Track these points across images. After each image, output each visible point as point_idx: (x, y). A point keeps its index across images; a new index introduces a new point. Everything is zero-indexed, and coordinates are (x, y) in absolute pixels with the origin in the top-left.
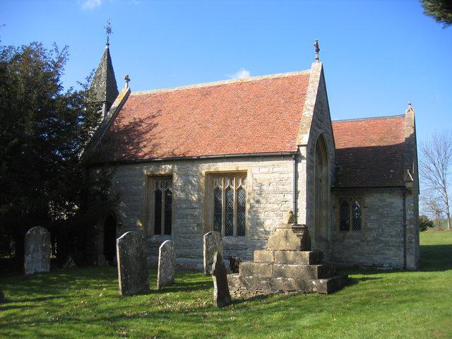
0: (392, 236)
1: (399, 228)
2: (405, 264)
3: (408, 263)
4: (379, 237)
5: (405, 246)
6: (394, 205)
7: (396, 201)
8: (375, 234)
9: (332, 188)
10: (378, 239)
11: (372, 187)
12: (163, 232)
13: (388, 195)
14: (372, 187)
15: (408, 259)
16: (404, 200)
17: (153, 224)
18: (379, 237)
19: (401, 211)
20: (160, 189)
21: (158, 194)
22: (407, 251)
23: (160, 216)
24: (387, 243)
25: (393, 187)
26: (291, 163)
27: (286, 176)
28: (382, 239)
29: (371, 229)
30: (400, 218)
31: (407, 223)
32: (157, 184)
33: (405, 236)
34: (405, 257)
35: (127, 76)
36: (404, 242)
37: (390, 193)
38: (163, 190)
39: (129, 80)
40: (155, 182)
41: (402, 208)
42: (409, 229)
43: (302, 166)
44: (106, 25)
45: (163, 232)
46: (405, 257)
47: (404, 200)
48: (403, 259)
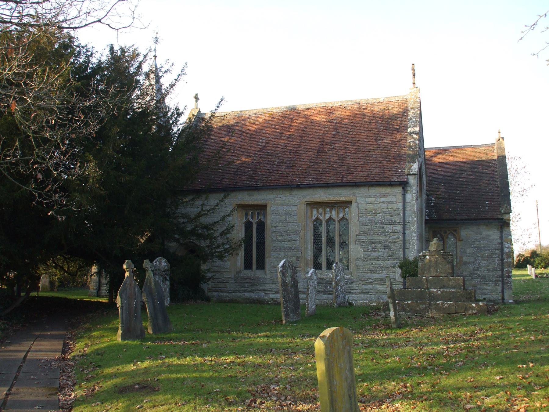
0: (489, 270)
1: (497, 261)
2: (503, 299)
3: (506, 298)
4: (476, 272)
5: (503, 281)
6: (491, 238)
7: (493, 234)
8: (471, 268)
9: (426, 220)
10: (474, 274)
11: (468, 219)
12: (254, 266)
13: (485, 227)
14: (468, 219)
15: (506, 294)
16: (501, 232)
17: (243, 258)
18: (476, 272)
19: (499, 244)
20: (251, 220)
21: (248, 226)
22: (505, 286)
23: (251, 250)
24: (483, 278)
25: (490, 219)
26: (398, 190)
27: (395, 206)
28: (479, 273)
29: (466, 263)
30: (497, 251)
31: (505, 256)
32: (247, 215)
33: (502, 270)
34: (503, 291)
35: (197, 95)
36: (502, 276)
37: (487, 226)
38: (254, 221)
39: (198, 99)
40: (244, 213)
41: (499, 241)
42: (507, 262)
43: (411, 196)
44: (154, 35)
45: (254, 266)
46: (503, 291)
47: (501, 232)
48: (500, 294)
